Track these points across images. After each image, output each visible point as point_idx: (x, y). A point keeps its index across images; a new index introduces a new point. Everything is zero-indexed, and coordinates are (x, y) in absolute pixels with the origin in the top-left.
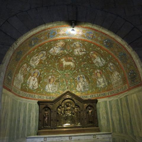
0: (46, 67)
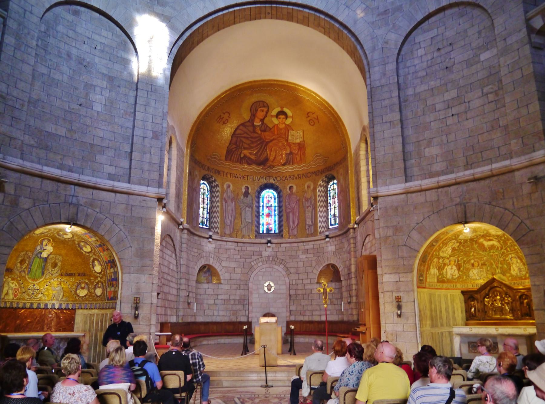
0: (462, 251)
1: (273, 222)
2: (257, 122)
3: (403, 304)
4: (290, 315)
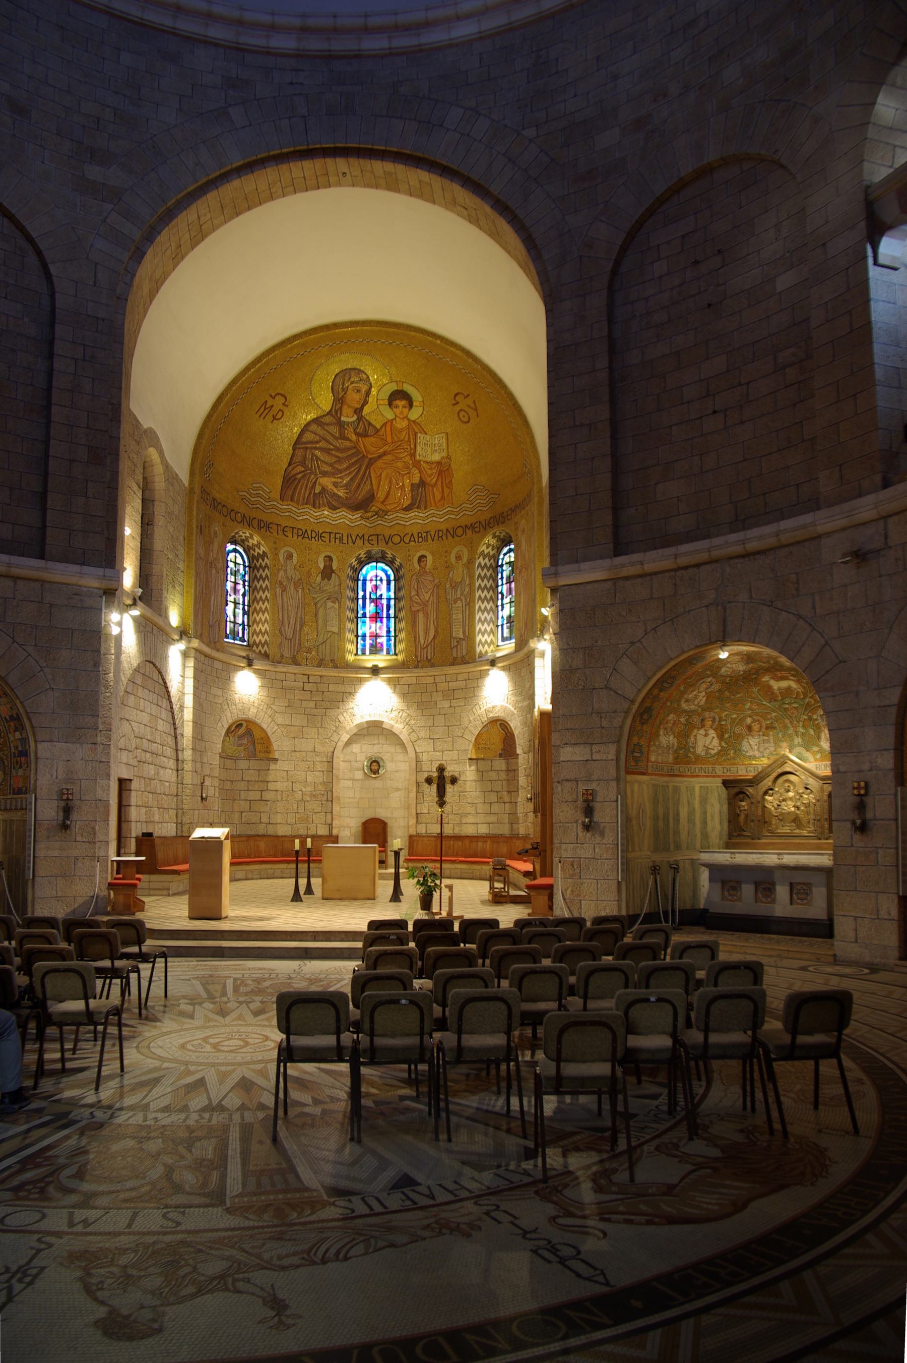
1: (384, 633)
2: (348, 417)
3: (597, 805)
4: (417, 822)
